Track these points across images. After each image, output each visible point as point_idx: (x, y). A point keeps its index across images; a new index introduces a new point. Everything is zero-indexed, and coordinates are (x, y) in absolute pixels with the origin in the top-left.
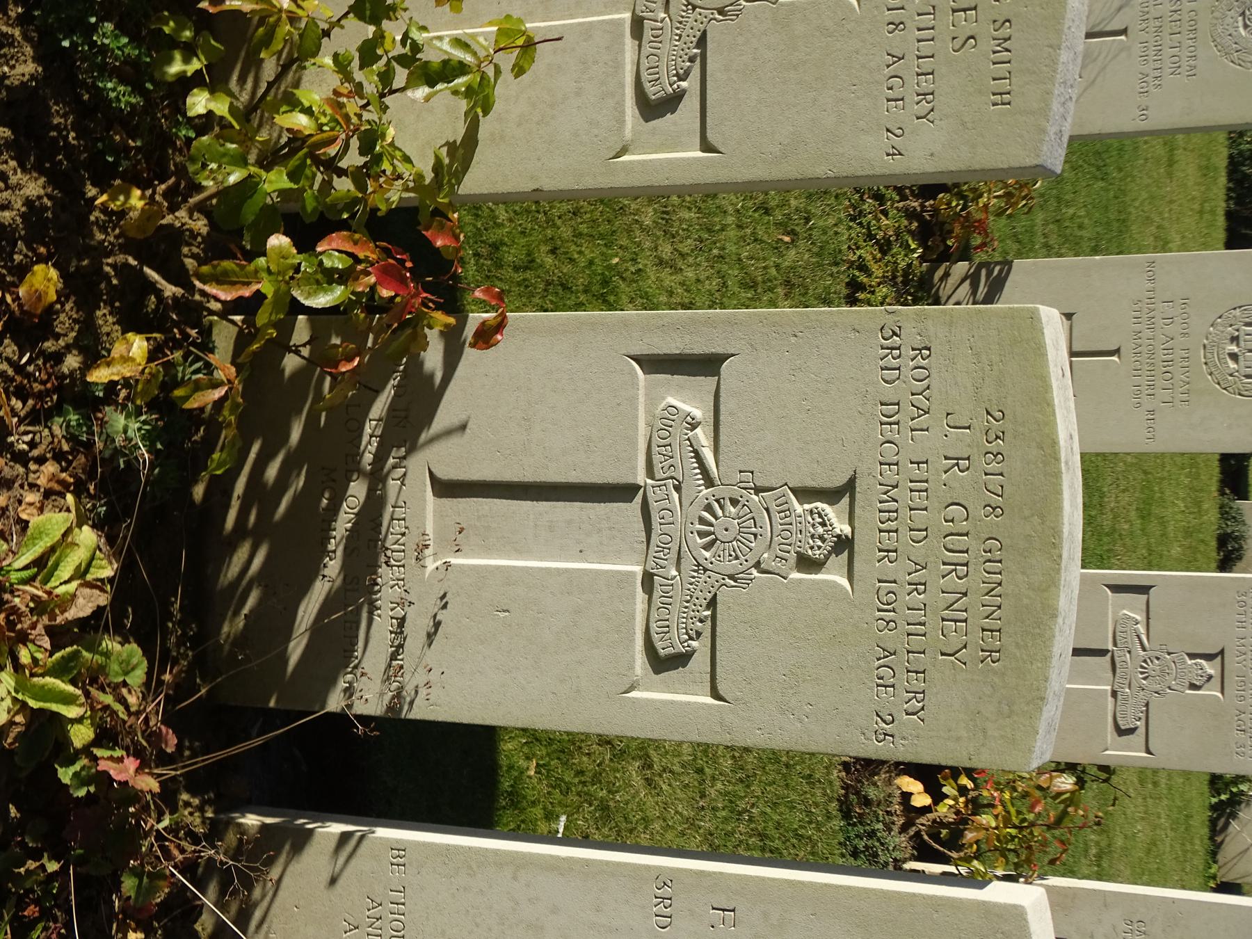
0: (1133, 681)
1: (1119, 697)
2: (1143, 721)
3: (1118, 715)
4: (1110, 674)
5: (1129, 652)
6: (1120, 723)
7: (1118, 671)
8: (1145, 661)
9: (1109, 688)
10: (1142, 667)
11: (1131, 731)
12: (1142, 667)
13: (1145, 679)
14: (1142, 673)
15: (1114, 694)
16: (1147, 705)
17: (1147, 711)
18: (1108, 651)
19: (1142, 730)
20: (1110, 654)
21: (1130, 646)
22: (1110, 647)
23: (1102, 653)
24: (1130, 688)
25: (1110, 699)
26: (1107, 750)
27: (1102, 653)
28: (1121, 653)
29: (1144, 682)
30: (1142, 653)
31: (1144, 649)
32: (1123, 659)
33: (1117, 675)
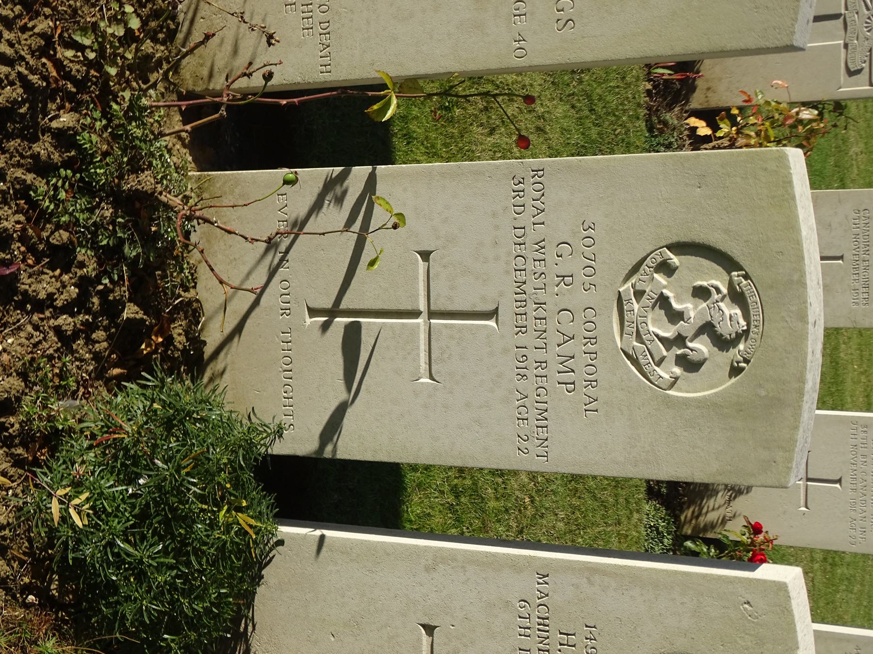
0: (861, 35)
1: (850, 47)
2: (868, 63)
3: (849, 61)
4: (843, 32)
5: (857, 13)
6: (851, 66)
7: (849, 28)
8: (869, 18)
9: (842, 42)
10: (867, 23)
11: (858, 72)
12: (867, 23)
13: (868, 31)
14: (866, 27)
15: (846, 46)
16: (870, 51)
17: (871, 55)
18: (841, 15)
19: (867, 70)
20: (843, 17)
21: (858, 8)
22: (843, 11)
23: (836, 16)
24: (857, 40)
25: (843, 50)
26: (840, 88)
27: (836, 16)
28: (851, 15)
29: (868, 34)
30: (866, 12)
31: (868, 9)
32: (853, 18)
33: (848, 31)
